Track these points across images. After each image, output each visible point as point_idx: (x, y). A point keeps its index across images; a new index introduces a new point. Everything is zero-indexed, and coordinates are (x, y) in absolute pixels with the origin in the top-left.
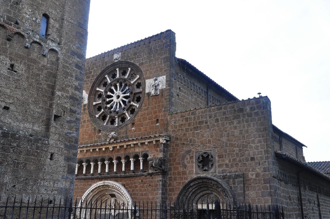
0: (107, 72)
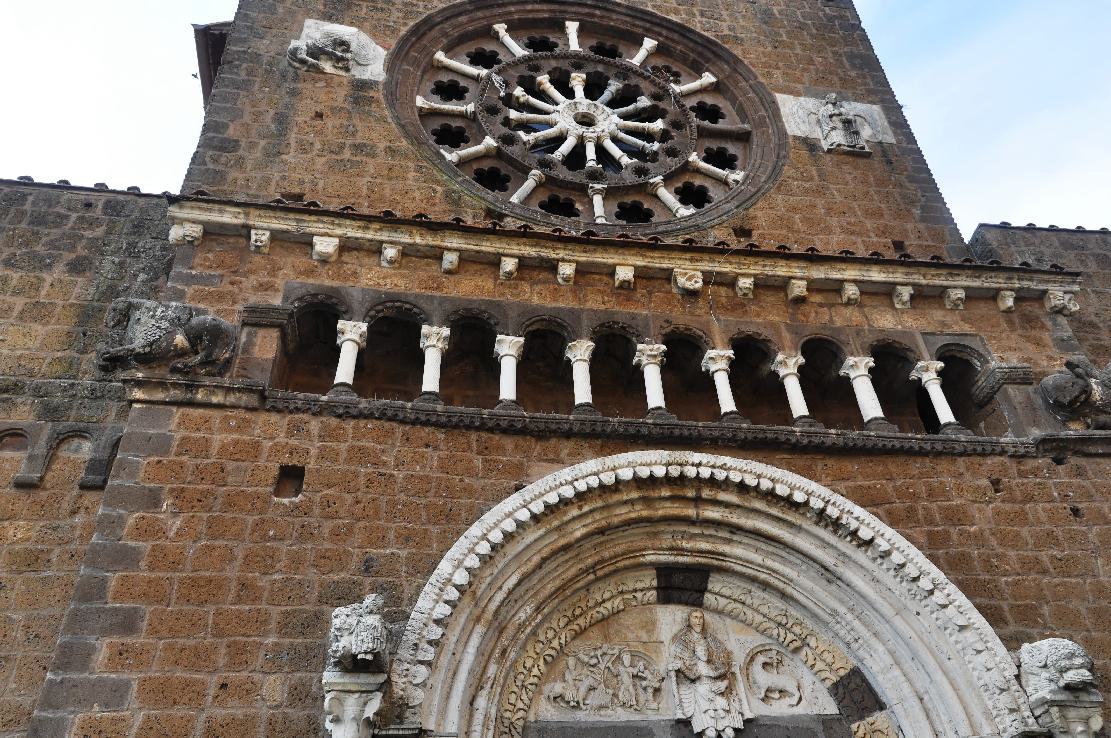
0: (510, 13)
